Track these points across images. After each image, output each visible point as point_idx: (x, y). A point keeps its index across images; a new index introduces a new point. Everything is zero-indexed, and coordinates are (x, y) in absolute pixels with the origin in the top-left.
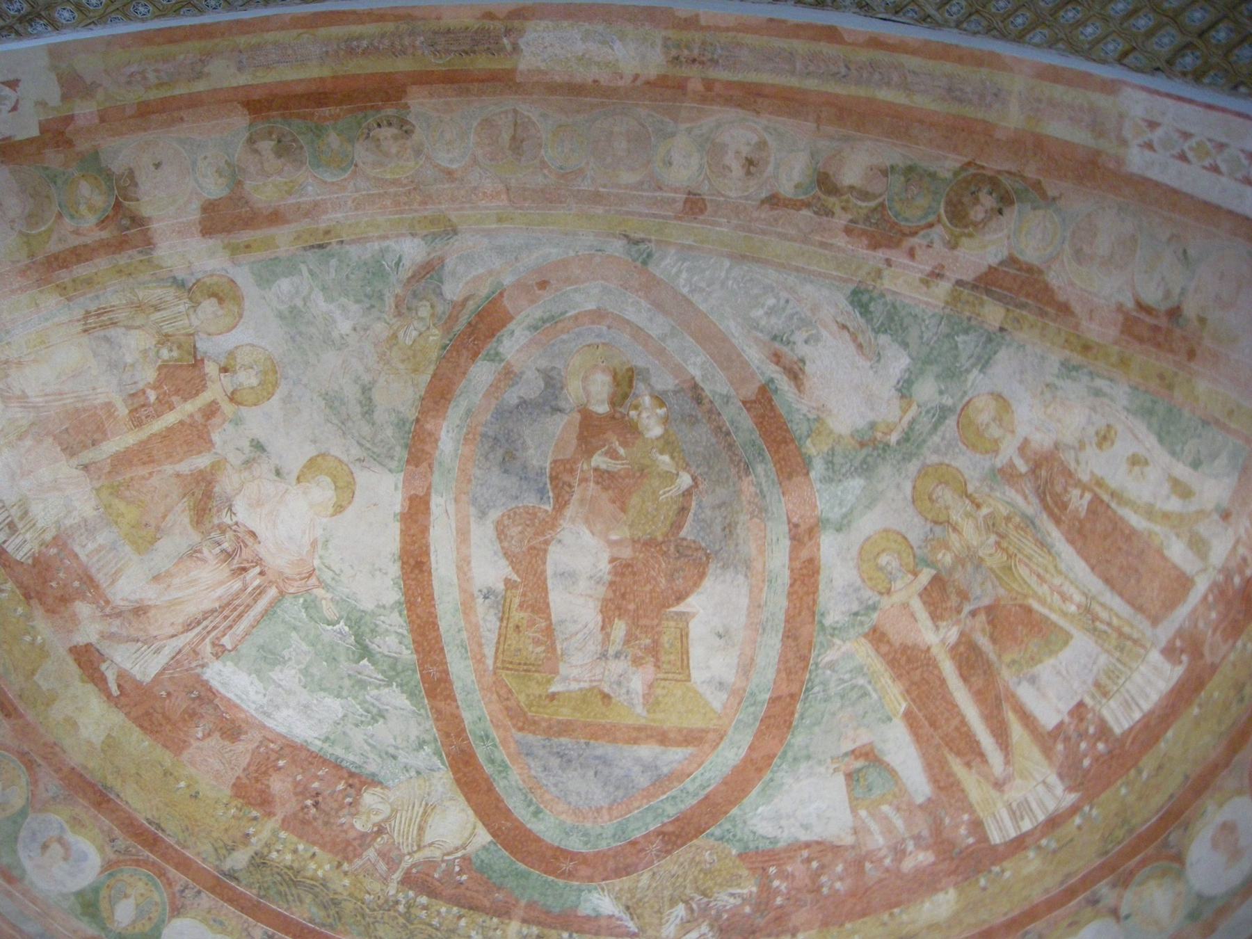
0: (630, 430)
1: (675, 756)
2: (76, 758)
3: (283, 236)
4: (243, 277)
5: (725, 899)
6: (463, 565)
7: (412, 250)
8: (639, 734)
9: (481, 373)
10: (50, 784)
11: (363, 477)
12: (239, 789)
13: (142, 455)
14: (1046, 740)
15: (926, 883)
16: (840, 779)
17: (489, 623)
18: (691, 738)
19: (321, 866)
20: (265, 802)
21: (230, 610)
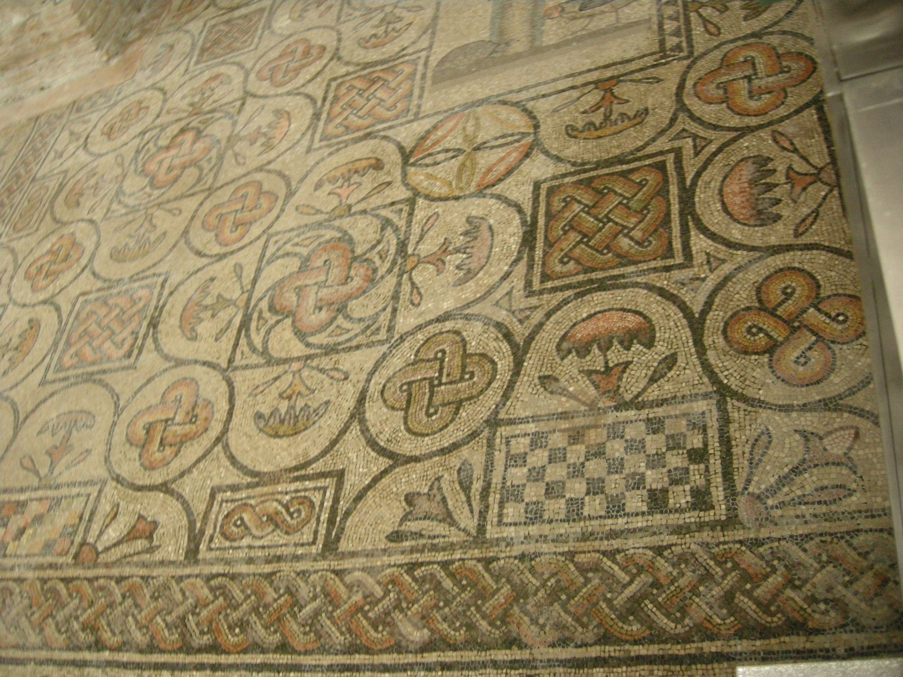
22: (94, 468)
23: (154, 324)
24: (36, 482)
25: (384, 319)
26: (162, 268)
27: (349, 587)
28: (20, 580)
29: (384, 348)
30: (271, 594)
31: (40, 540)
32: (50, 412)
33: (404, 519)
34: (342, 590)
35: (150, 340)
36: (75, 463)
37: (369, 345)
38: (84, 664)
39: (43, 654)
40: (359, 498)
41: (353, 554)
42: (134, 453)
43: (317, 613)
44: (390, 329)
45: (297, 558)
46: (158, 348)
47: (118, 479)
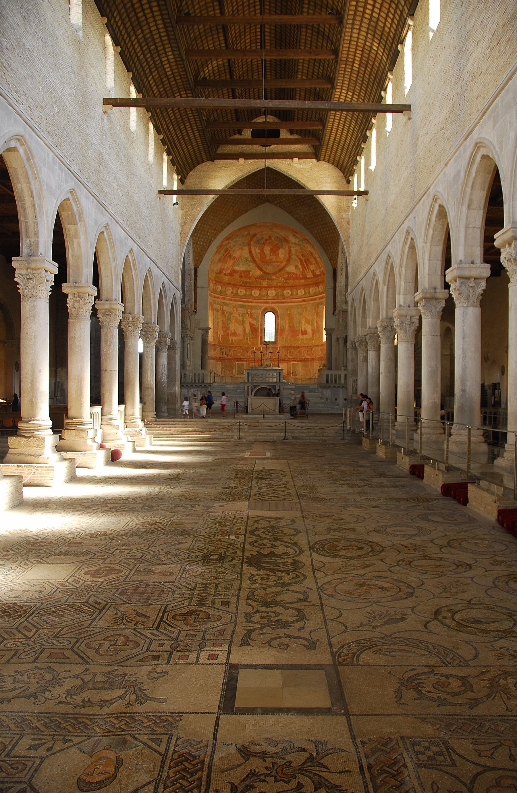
0: (271, 239)
1: (279, 264)
2: (227, 282)
3: (234, 237)
4: (230, 241)
5: (285, 277)
6: (255, 252)
7: (246, 233)
8: (275, 262)
9: (255, 238)
10: (226, 286)
11: (244, 248)
12: (240, 277)
13: (225, 257)
14: (312, 271)
15: (302, 279)
16: (294, 268)
17: (259, 255)
18: (280, 262)
19: (248, 280)
20: (242, 277)
21: (234, 263)
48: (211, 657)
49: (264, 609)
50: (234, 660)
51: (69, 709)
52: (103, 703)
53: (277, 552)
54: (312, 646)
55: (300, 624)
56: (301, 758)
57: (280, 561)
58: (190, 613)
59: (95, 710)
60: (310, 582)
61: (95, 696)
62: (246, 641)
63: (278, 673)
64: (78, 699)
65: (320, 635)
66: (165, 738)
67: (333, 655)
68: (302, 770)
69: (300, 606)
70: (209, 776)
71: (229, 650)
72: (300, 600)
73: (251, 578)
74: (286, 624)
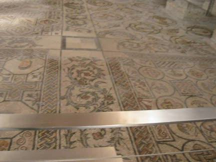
22: (157, 95)
23: (191, 96)
24: (150, 85)
25: (213, 140)
26: (205, 94)
27: (152, 148)
28: (131, 90)
29: (206, 142)
30: (145, 134)
31: (139, 91)
32: (164, 84)
33: (170, 156)
34: (150, 147)
35: (187, 97)
36: (156, 92)
37: (206, 139)
38: (120, 105)
39: (119, 98)
40: (172, 146)
41: (159, 147)
42: (163, 101)
43: (144, 144)
44: (212, 142)
45: (154, 136)
46: (187, 99)
47: (157, 100)
48: (56, 34)
49: (72, 20)
50: (64, 34)
51: (10, 48)
52: (21, 47)
53: (75, 2)
54: (89, 32)
55: (85, 25)
56: (88, 62)
57: (76, 6)
58: (47, 20)
59: (20, 49)
60: (87, 13)
61: (18, 45)
62: (67, 29)
63: (79, 39)
64: (13, 45)
65: (92, 29)
66: (45, 56)
67: (97, 35)
68: (89, 64)
69: (85, 20)
70: (61, 66)
71: (62, 32)
72: (84, 18)
73: (66, 10)
74: (80, 25)
